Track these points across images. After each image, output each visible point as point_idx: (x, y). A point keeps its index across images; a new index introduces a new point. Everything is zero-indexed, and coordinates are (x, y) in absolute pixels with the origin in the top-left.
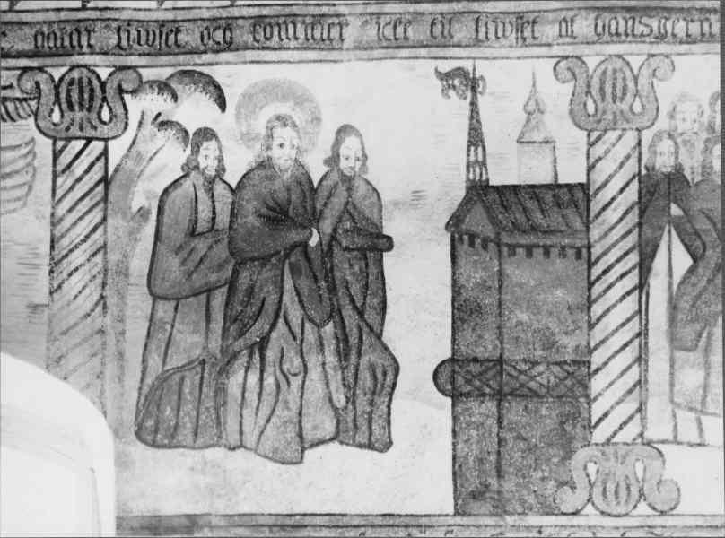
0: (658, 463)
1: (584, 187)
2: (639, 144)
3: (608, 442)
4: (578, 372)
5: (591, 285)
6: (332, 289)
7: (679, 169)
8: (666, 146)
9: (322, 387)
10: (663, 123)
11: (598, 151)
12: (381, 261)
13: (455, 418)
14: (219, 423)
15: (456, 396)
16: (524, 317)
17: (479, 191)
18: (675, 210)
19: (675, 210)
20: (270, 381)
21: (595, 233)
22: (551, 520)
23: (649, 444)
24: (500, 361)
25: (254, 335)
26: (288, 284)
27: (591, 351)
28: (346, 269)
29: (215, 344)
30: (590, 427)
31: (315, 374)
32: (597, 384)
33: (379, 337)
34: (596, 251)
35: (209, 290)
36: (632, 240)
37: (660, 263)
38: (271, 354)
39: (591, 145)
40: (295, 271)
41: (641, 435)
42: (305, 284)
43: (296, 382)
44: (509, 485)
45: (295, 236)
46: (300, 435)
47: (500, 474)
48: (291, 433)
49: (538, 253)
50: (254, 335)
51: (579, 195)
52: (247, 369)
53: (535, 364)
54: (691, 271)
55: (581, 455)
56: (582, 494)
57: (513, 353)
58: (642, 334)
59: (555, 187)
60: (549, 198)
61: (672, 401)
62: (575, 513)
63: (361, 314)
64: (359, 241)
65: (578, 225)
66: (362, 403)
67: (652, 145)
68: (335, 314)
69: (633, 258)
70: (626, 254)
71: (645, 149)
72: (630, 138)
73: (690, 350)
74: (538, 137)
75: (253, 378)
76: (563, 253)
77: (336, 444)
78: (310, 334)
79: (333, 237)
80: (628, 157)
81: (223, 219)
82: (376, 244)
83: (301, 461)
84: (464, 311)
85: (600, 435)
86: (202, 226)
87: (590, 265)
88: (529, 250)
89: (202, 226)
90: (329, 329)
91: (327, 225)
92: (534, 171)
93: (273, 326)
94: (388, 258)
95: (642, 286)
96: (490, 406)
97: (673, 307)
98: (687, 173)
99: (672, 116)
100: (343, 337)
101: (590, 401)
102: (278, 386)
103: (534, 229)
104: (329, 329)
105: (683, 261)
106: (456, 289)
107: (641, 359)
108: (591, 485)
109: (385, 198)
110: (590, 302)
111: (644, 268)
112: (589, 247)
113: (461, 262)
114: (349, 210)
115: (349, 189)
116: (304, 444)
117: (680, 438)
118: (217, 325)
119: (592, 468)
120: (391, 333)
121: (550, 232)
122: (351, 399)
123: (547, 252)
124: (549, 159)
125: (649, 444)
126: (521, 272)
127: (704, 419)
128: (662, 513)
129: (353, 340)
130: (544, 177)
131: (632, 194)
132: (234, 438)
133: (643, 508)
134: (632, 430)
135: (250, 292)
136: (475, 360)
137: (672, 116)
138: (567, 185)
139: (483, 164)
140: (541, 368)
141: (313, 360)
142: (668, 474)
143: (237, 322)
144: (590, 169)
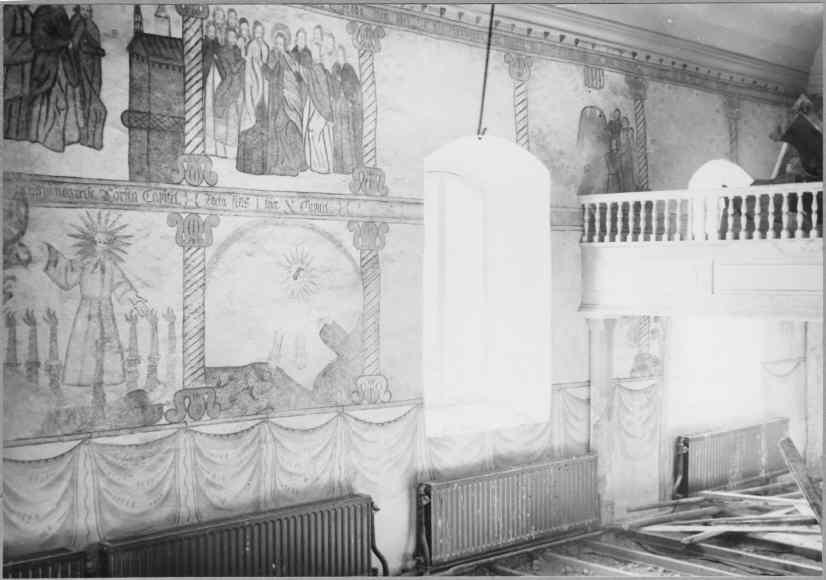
0: (209, 164)
1: (181, 40)
2: (202, 26)
3: (191, 154)
4: (180, 123)
5: (185, 84)
6: (79, 71)
7: (216, 39)
8: (212, 28)
9: (73, 120)
10: (211, 18)
11: (187, 25)
12: (100, 61)
13: (130, 137)
14: (28, 129)
15: (130, 128)
16: (159, 95)
17: (139, 35)
18: (215, 56)
19: (215, 56)
20: (51, 114)
21: (186, 62)
22: (167, 186)
23: (205, 155)
24: (149, 113)
25: (45, 87)
26: (61, 66)
27: (185, 113)
28: (85, 62)
29: (26, 91)
30: (185, 147)
31: (71, 110)
32: (188, 128)
33: (98, 96)
34: (187, 69)
35: (23, 63)
36: (199, 67)
37: (210, 79)
38: (53, 99)
39: (184, 22)
40: (64, 60)
41: (203, 152)
42: (68, 67)
43: (63, 113)
44: (153, 169)
45: (61, 43)
46: (64, 139)
47: (148, 164)
48: (59, 137)
49: (164, 67)
50: (45, 87)
51: (179, 43)
52: (42, 104)
53: (164, 116)
54: (221, 84)
55: (181, 158)
56: (181, 176)
57: (155, 111)
58: (203, 109)
59: (170, 38)
60: (167, 42)
61: (214, 138)
62: (179, 184)
63: (90, 83)
64: (92, 50)
65: (179, 57)
66: (91, 128)
67: (207, 27)
68: (80, 82)
69: (200, 75)
70: (198, 73)
71: (204, 28)
72: (198, 23)
73: (220, 117)
74: (163, 15)
75: (44, 109)
76: (174, 69)
77: (78, 146)
78: (70, 91)
79: (79, 44)
80: (198, 31)
81: (28, 30)
82: (99, 53)
83: (63, 150)
84: (134, 90)
85: (189, 150)
86: (18, 31)
87: (185, 75)
88: (160, 65)
89: (18, 31)
90: (77, 90)
91: (76, 40)
92: (161, 30)
93: (53, 85)
94: (104, 61)
95: (203, 88)
96: (145, 133)
97: (215, 99)
98: (220, 41)
99: (214, 15)
100: (83, 94)
101: (185, 135)
102: (55, 113)
103: (161, 56)
104: (77, 90)
105: (218, 79)
106: (131, 78)
107: (203, 119)
108: (185, 171)
109: (102, 31)
110: (184, 92)
111: (204, 79)
112: (184, 67)
113: (134, 65)
114: (85, 34)
115: (85, 25)
116: (65, 143)
117: (219, 154)
118: (27, 81)
119: (185, 164)
120: (104, 95)
121: (167, 59)
122: (86, 125)
123: (167, 68)
124: (167, 27)
125: (205, 155)
126: (158, 76)
127: (227, 147)
128: (212, 186)
129: (88, 97)
130: (165, 33)
131: (199, 47)
132: (34, 138)
133: (204, 184)
134: (199, 151)
135: (43, 67)
136: (139, 112)
137: (214, 15)
138: (175, 39)
139: (141, 23)
140: (165, 119)
141: (71, 104)
142: (213, 170)
143: (37, 81)
144: (184, 32)
